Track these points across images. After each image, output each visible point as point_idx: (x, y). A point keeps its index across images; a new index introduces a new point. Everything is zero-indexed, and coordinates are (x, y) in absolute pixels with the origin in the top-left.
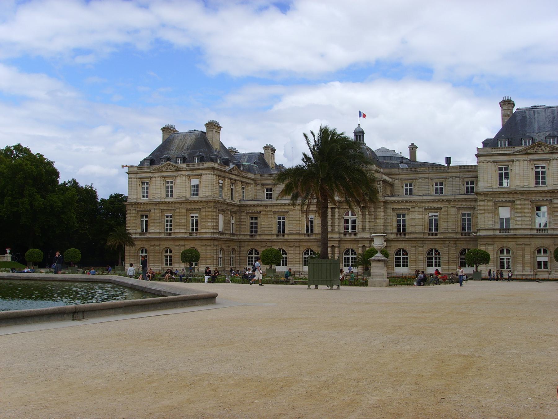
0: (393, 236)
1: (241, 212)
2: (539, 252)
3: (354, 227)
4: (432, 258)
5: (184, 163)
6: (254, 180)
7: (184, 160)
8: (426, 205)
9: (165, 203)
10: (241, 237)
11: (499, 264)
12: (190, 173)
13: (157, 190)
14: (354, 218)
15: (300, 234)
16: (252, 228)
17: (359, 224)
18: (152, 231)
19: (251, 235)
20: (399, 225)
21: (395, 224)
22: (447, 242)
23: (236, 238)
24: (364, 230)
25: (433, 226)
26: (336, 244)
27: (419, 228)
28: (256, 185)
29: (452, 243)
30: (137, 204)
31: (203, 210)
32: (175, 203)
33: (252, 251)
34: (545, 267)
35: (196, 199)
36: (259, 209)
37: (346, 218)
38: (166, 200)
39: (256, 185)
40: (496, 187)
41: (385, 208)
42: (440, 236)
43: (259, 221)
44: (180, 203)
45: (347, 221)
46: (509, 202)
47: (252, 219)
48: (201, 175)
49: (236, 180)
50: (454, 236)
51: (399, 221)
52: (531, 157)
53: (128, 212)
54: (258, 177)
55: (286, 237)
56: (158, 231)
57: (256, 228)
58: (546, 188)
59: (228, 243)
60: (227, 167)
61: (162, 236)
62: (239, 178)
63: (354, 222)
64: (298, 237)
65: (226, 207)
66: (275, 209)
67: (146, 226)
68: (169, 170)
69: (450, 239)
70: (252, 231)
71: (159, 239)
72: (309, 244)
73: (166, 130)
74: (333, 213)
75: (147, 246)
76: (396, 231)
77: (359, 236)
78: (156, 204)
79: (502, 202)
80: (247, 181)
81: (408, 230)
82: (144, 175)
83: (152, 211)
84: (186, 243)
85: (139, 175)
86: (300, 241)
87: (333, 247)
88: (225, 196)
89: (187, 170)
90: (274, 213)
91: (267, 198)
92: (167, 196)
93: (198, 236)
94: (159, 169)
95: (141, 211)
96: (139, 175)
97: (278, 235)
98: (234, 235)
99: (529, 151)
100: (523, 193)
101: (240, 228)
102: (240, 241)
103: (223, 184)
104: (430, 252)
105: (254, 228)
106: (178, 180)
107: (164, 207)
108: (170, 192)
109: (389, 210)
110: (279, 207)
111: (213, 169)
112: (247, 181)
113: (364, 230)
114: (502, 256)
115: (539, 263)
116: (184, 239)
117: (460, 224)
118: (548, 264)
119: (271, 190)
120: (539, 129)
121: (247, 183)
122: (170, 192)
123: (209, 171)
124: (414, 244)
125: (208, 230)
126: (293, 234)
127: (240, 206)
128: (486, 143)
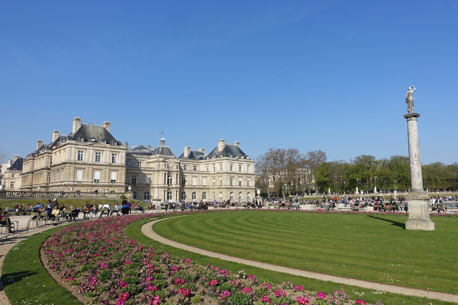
8: (193, 175)
12: (112, 150)
35: (114, 164)
44: (106, 166)
56: (91, 181)
61: (93, 184)
68: (99, 146)
78: (90, 165)
92: (96, 161)
94: (92, 145)
96: (77, 146)
106: (105, 152)
107: (95, 167)
122: (98, 158)
123: (124, 151)
124: (189, 190)
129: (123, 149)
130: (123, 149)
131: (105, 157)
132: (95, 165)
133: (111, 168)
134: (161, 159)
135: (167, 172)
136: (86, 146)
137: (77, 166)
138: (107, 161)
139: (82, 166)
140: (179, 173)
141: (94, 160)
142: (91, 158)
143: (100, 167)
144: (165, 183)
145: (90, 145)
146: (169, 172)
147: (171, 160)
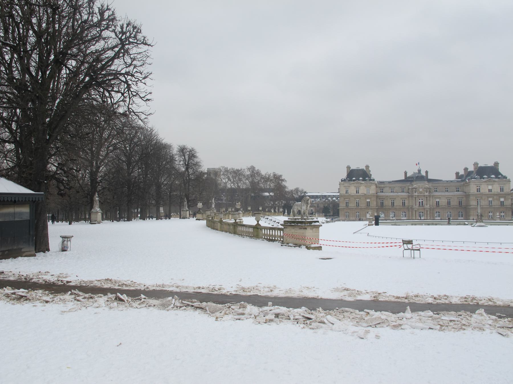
13: (352, 190)
25: (449, 203)
43: (384, 201)
63: (422, 202)
73: (348, 167)
74: (416, 199)
75: (349, 211)
78: (352, 196)
81: (440, 204)
87: (416, 211)
100: (485, 195)
105: (382, 204)
106: (361, 188)
108: (357, 192)
116: (364, 209)
122: (357, 192)
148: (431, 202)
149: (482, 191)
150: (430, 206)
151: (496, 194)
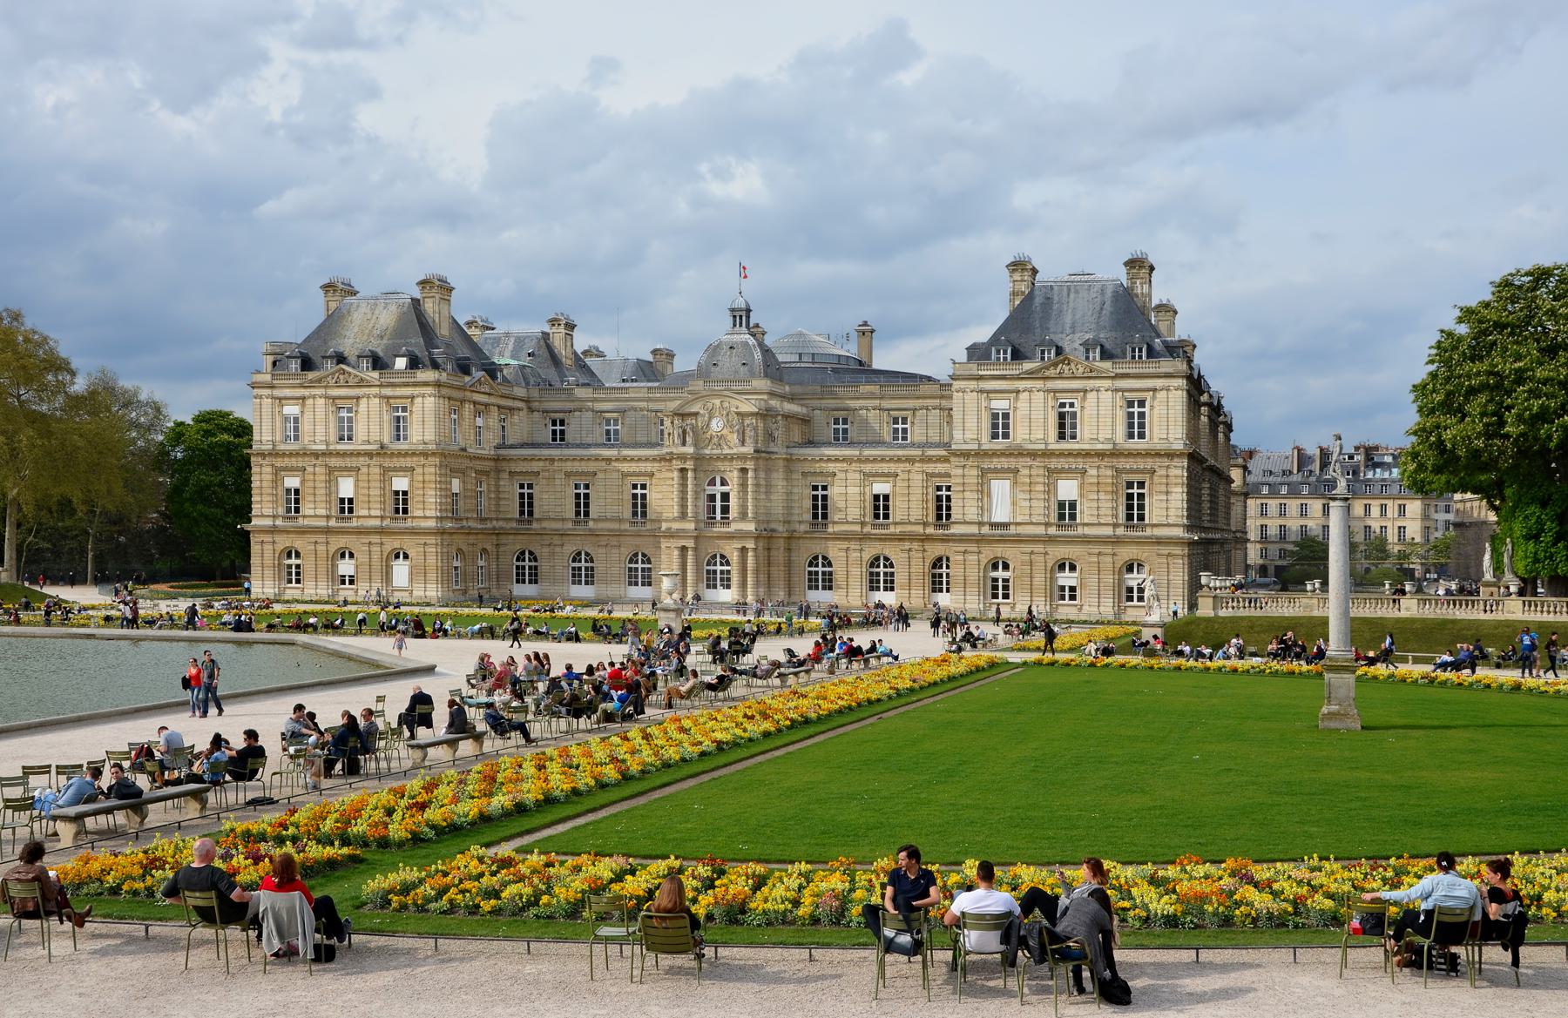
0: (803, 528)
1: (498, 471)
2: (1062, 567)
3: (725, 510)
4: (878, 574)
5: (374, 369)
6: (527, 401)
7: (378, 363)
8: (868, 468)
9: (338, 454)
10: (501, 523)
11: (989, 592)
12: (388, 392)
14: (725, 489)
15: (620, 520)
16: (522, 505)
17: (733, 503)
18: (311, 512)
19: (519, 521)
20: (815, 507)
21: (809, 503)
22: (907, 545)
23: (489, 525)
24: (743, 516)
25: (881, 506)
26: (690, 543)
27: (854, 513)
28: (531, 410)
29: (915, 545)
30: (274, 454)
31: (419, 470)
32: (359, 454)
33: (523, 553)
34: (1073, 598)
35: (402, 446)
36: (536, 466)
37: (710, 490)
38: (339, 447)
39: (531, 410)
40: (987, 444)
41: (789, 471)
42: (892, 529)
43: (536, 491)
44: (369, 454)
45: (712, 498)
46: (1009, 470)
47: (522, 486)
48: (413, 398)
49: (486, 405)
50: (920, 529)
51: (815, 498)
52: (1051, 384)
53: (255, 469)
54: (535, 393)
55: (591, 524)
56: (323, 512)
57: (531, 505)
58: (1076, 446)
59: (472, 539)
60: (467, 379)
62: (493, 400)
63: (725, 497)
64: (615, 526)
65: (467, 463)
66: (569, 466)
67: (297, 501)
69: (911, 537)
70: (522, 513)
71: (328, 531)
72: (638, 541)
76: (808, 517)
77: (734, 527)
78: (316, 455)
79: (996, 471)
80: (509, 403)
81: (835, 516)
82: (288, 392)
83: (310, 469)
84: (385, 539)
85: (277, 393)
86: (620, 534)
87: (684, 549)
88: (465, 437)
89: (381, 386)
90: (568, 475)
91: (554, 439)
92: (341, 439)
93: (409, 523)
94: (320, 381)
95: (286, 469)
96: (277, 393)
97: (577, 522)
98: (483, 520)
99: (1047, 373)
100: (1033, 454)
101: (498, 505)
102: (497, 533)
103: (461, 416)
104: (874, 562)
105: (527, 504)
107: (333, 462)
109: (795, 476)
110: (576, 464)
111: (438, 384)
112: (509, 403)
113: (743, 516)
114: (994, 574)
115: (1062, 588)
117: (932, 506)
118: (1078, 593)
119: (562, 423)
120: (1073, 327)
121: (511, 409)
123: (429, 390)
124: (845, 545)
125: (428, 513)
126: (606, 520)
127: (497, 459)
128: (977, 353)
129: (426, 384)
130: (426, 384)
131: (371, 423)
132: (328, 454)
133: (387, 463)
134: (673, 405)
135: (689, 465)
136: (302, 386)
137: (279, 463)
138: (375, 436)
139: (293, 462)
140: (750, 465)
141: (333, 437)
142: (320, 429)
143: (349, 462)
144: (683, 516)
145: (311, 381)
146: (698, 459)
147: (717, 402)
148: (778, 497)
149: (1020, 434)
150: (763, 520)
151: (1101, 455)
